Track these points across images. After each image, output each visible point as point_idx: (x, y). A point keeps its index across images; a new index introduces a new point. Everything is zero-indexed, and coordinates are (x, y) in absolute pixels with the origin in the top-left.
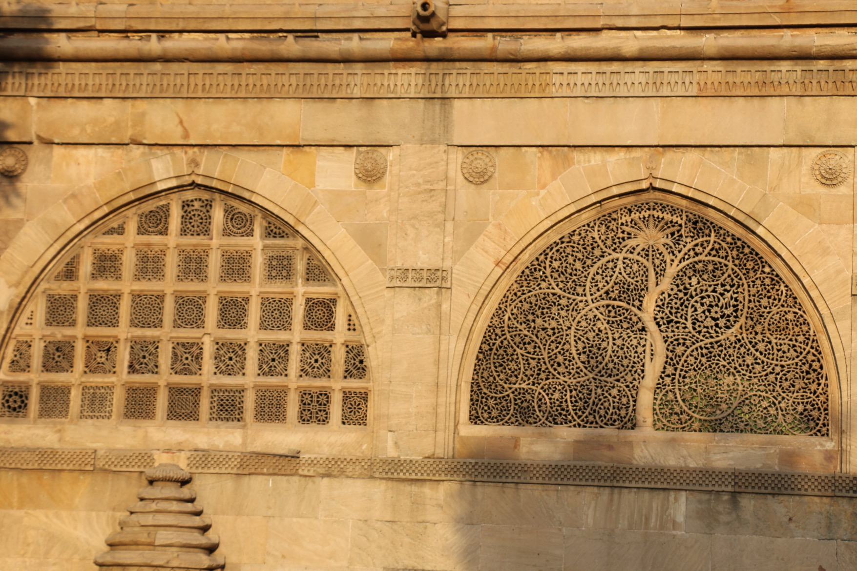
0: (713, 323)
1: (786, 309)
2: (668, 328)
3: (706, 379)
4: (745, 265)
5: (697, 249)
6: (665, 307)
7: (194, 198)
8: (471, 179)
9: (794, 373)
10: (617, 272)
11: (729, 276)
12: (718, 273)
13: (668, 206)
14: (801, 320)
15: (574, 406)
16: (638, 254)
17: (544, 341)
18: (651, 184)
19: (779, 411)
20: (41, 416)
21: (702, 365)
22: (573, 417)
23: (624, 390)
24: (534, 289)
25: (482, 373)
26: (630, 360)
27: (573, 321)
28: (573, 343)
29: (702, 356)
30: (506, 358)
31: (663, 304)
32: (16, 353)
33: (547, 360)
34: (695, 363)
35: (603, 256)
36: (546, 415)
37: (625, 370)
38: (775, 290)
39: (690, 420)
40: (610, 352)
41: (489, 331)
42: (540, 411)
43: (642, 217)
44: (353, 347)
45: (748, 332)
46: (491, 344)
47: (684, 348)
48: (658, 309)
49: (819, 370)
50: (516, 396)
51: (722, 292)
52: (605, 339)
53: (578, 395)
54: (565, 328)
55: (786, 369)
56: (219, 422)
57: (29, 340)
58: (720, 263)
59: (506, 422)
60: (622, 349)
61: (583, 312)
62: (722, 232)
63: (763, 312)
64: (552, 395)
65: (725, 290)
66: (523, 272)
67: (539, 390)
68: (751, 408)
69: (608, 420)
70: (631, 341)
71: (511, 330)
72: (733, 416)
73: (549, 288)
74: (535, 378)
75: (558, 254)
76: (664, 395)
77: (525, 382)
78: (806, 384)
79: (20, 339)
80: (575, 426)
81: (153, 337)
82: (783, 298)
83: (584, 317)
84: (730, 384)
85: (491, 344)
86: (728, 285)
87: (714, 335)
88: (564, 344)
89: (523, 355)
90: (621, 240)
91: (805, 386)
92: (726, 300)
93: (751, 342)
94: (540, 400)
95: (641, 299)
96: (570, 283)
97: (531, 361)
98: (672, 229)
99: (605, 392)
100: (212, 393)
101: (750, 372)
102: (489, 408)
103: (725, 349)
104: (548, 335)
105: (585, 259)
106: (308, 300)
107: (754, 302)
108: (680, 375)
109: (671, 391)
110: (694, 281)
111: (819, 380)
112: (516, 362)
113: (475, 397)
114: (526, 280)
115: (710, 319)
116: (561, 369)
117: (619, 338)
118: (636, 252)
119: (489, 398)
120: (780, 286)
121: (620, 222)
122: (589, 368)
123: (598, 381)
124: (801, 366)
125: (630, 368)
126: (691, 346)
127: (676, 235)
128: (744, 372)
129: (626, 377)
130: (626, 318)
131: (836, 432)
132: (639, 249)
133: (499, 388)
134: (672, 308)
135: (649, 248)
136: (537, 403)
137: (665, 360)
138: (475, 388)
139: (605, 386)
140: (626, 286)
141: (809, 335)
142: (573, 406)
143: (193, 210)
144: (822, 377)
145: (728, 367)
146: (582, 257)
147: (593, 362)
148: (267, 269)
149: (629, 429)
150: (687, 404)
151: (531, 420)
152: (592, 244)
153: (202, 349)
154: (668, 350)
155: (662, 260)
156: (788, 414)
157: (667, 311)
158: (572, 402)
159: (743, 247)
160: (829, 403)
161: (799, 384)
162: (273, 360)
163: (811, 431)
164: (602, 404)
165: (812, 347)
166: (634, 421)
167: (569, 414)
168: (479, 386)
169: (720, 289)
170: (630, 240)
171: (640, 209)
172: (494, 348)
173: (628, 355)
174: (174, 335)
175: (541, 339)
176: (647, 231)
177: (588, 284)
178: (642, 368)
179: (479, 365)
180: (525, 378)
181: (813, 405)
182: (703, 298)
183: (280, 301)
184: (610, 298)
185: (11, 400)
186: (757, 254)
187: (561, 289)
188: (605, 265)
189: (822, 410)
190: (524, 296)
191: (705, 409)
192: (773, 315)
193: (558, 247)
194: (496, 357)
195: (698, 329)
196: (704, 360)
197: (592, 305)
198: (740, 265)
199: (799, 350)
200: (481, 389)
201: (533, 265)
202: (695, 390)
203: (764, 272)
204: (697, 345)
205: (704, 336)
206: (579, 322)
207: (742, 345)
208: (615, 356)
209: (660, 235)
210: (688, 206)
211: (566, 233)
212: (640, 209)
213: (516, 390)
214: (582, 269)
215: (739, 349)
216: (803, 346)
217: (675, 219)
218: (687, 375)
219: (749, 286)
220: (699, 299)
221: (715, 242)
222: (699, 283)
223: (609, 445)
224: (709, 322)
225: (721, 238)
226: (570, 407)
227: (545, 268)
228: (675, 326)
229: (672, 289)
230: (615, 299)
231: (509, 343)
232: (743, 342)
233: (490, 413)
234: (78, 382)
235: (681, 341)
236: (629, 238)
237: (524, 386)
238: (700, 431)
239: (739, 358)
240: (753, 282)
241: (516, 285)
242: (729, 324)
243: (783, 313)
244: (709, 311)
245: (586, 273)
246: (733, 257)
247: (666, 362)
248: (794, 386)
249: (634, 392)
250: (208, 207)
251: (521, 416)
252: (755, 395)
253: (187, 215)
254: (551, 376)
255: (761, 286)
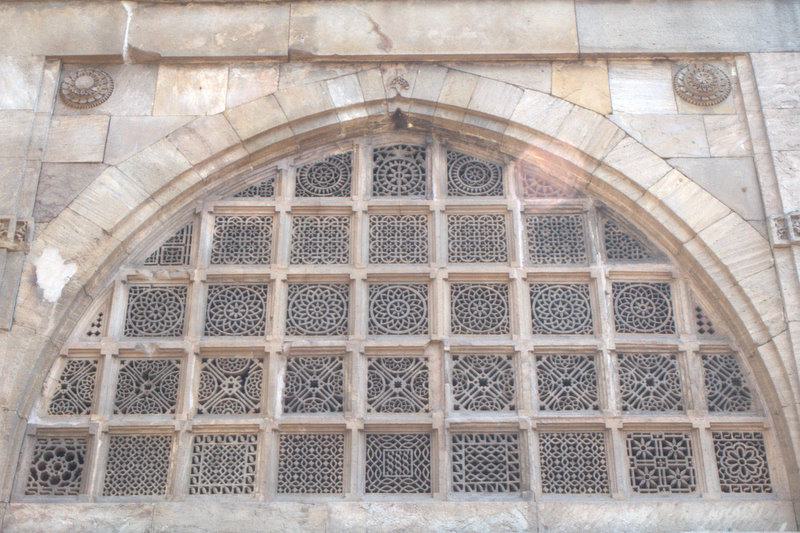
7: (393, 144)
20: (108, 490)
32: (65, 382)
44: (715, 359)
56: (474, 494)
57: (91, 361)
79: (76, 358)
81: (331, 348)
100: (454, 441)
106: (617, 287)
143: (393, 162)
148: (534, 242)
153: (425, 368)
162: (567, 383)
174: (372, 343)
183: (564, 290)
185: (48, 470)
234: (187, 427)
250: (419, 157)
253: (383, 168)
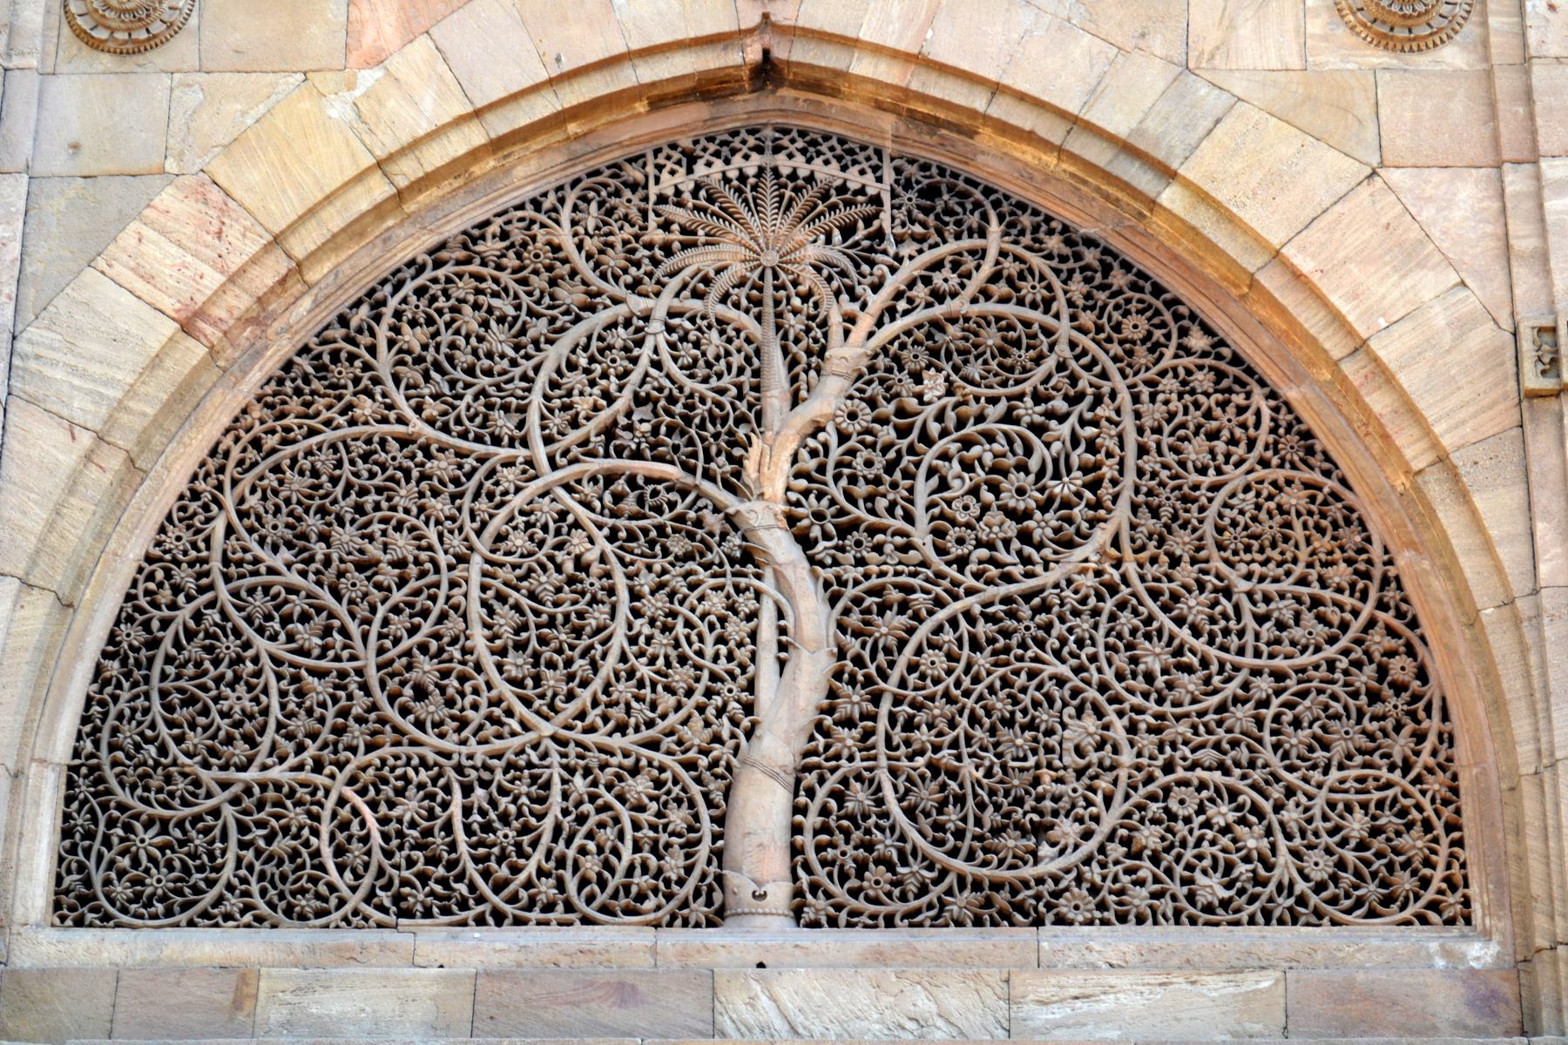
0: (1011, 528)
1: (1281, 475)
2: (842, 549)
3: (993, 731)
4: (1117, 328)
5: (937, 278)
6: (829, 478)
8: (101, 34)
9: (1323, 698)
10: (644, 362)
11: (1061, 367)
12: (1022, 356)
13: (827, 138)
14: (1336, 510)
15: (481, 844)
16: (724, 299)
17: (362, 610)
18: (766, 53)
19: (1279, 837)
21: (976, 680)
22: (472, 887)
23: (676, 782)
24: (328, 423)
25: (115, 731)
26: (698, 668)
27: (479, 533)
28: (476, 611)
29: (976, 646)
30: (213, 673)
31: (821, 469)
33: (373, 677)
34: (949, 672)
35: (592, 309)
36: (367, 881)
37: (679, 707)
38: (1231, 409)
39: (936, 882)
40: (619, 641)
41: (151, 577)
42: (341, 869)
43: (733, 174)
45: (1144, 555)
46: (155, 624)
47: (904, 620)
48: (803, 483)
49: (1416, 685)
50: (246, 812)
51: (1039, 419)
52: (601, 595)
53: (493, 803)
54: (443, 560)
55: (1292, 684)
58: (1027, 324)
59: (205, 915)
60: (666, 629)
61: (517, 502)
62: (1026, 220)
63: (1196, 487)
64: (391, 805)
65: (1050, 415)
66: (288, 366)
67: (340, 787)
68: (1169, 830)
69: (615, 896)
70: (701, 599)
71: (233, 569)
72: (1103, 866)
73: (384, 420)
74: (325, 746)
75: (424, 302)
76: (832, 794)
77: (282, 759)
78: (1371, 737)
80: (480, 921)
82: (1264, 436)
83: (520, 520)
84: (1089, 743)
85: (155, 624)
86: (1059, 396)
87: (1017, 571)
88: (443, 617)
89: (277, 661)
90: (658, 253)
91: (1364, 742)
92: (1056, 446)
93: (1155, 594)
94: (344, 826)
95: (737, 452)
96: (468, 398)
97: (310, 680)
98: (843, 215)
99: (602, 790)
101: (1160, 701)
102: (136, 863)
103: (1062, 620)
104: (379, 586)
105: (524, 317)
107: (1160, 453)
108: (893, 719)
109: (859, 778)
110: (934, 385)
111: (1418, 722)
112: (251, 688)
113: (81, 820)
114: (298, 392)
115: (1000, 516)
116: (432, 708)
117: (653, 593)
118: (715, 292)
119: (138, 826)
120: (1248, 395)
121: (653, 191)
122: (537, 703)
123: (572, 750)
124: (1346, 673)
125: (698, 697)
126: (931, 613)
127: (861, 232)
128: (1138, 700)
129: (685, 732)
130: (681, 519)
131: (1501, 906)
132: (722, 283)
133: (181, 785)
134: (853, 479)
135: (762, 277)
136: (332, 837)
137: (834, 665)
138: (84, 789)
139: (603, 766)
140: (678, 409)
141: (1369, 562)
142: (474, 846)
144: (1428, 709)
145: (1076, 681)
146: (511, 311)
147: (552, 679)
149: (698, 925)
150: (925, 823)
151: (301, 902)
152: (550, 269)
154: (842, 627)
155: (811, 318)
156: (1311, 847)
157: (836, 492)
158: (468, 831)
159: (1107, 270)
160: (1467, 802)
161: (1345, 737)
163: (1403, 908)
164: (590, 836)
165: (1382, 606)
166: (717, 897)
167: (460, 878)
168: (101, 780)
169: (1029, 411)
170: (690, 252)
171: (725, 151)
172: (168, 636)
173: (690, 653)
175: (351, 602)
176: (754, 222)
177: (536, 399)
178: (744, 696)
179: (102, 703)
180: (289, 747)
181: (1403, 813)
182: (967, 444)
184: (619, 452)
186: (1158, 290)
187: (431, 422)
188: (601, 338)
189: (1439, 829)
190: (289, 450)
191: (992, 842)
192: (1233, 496)
193: (421, 281)
194: (171, 670)
195: (956, 551)
196: (983, 660)
197: (549, 477)
198: (1099, 329)
199: (1335, 616)
200: (109, 792)
201: (325, 342)
202: (953, 774)
203: (1189, 352)
204: (955, 607)
205: (977, 576)
206: (501, 538)
207: (1122, 606)
208: (641, 654)
209: (802, 234)
210: (902, 130)
211: (452, 228)
212: (725, 148)
213: (248, 791)
214: (511, 353)
215: (1113, 618)
216: (1345, 598)
217: (854, 179)
218: (921, 717)
219: (1136, 399)
220: (954, 448)
221: (1003, 254)
222: (950, 392)
223: (621, 985)
224: (998, 526)
225: (1027, 240)
226: (463, 848)
227: (372, 350)
228: (867, 543)
229: (852, 416)
230: (637, 455)
231: (225, 616)
232: (1125, 591)
233: (135, 882)
235: (895, 595)
236: (685, 246)
237: (278, 773)
238: (978, 922)
239: (1116, 650)
240: (1150, 383)
241: (257, 412)
242: (1071, 530)
243: (1266, 489)
244: (995, 489)
245: (527, 366)
246: (1071, 304)
247: (838, 676)
248: (1326, 747)
249: (715, 787)
251: (263, 893)
252: (1185, 783)
254: (389, 735)
255: (1180, 396)
